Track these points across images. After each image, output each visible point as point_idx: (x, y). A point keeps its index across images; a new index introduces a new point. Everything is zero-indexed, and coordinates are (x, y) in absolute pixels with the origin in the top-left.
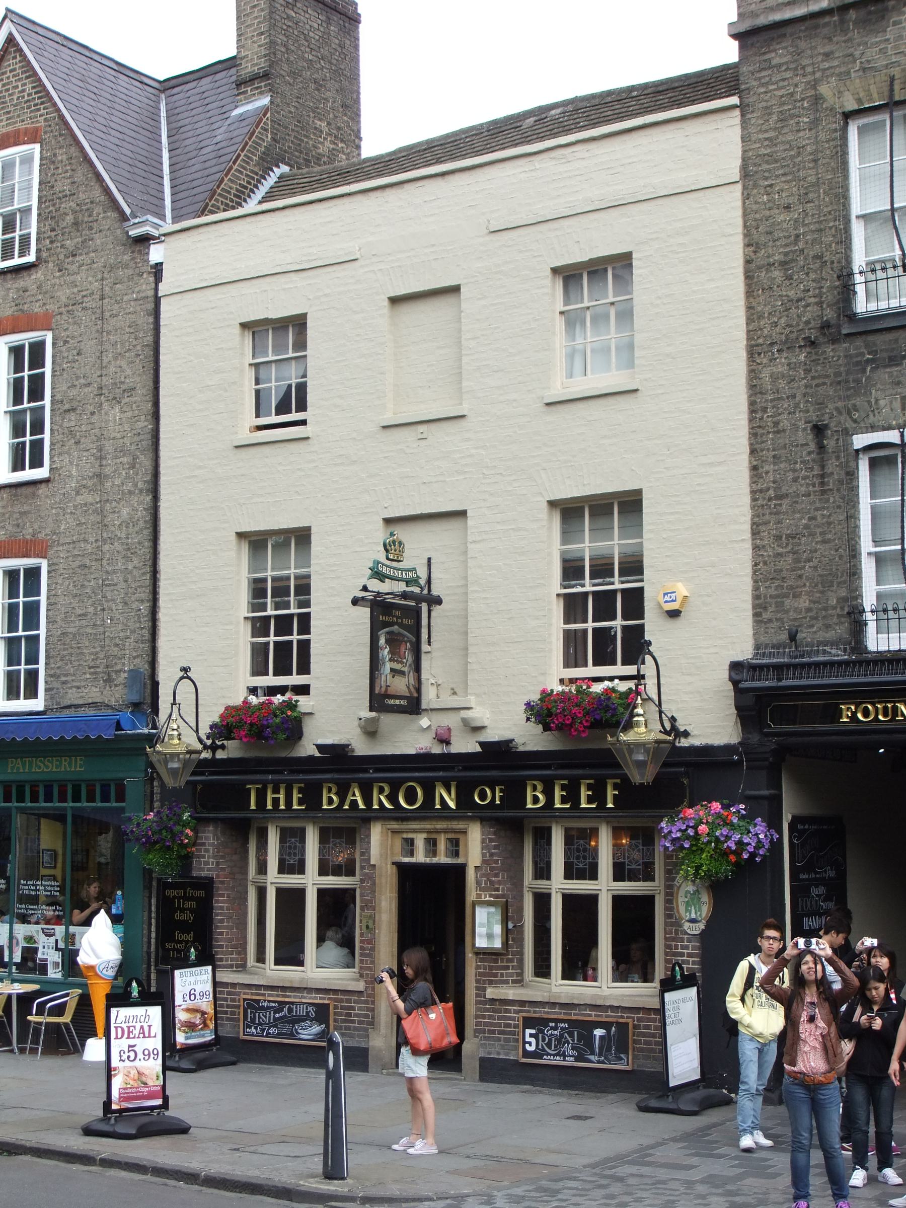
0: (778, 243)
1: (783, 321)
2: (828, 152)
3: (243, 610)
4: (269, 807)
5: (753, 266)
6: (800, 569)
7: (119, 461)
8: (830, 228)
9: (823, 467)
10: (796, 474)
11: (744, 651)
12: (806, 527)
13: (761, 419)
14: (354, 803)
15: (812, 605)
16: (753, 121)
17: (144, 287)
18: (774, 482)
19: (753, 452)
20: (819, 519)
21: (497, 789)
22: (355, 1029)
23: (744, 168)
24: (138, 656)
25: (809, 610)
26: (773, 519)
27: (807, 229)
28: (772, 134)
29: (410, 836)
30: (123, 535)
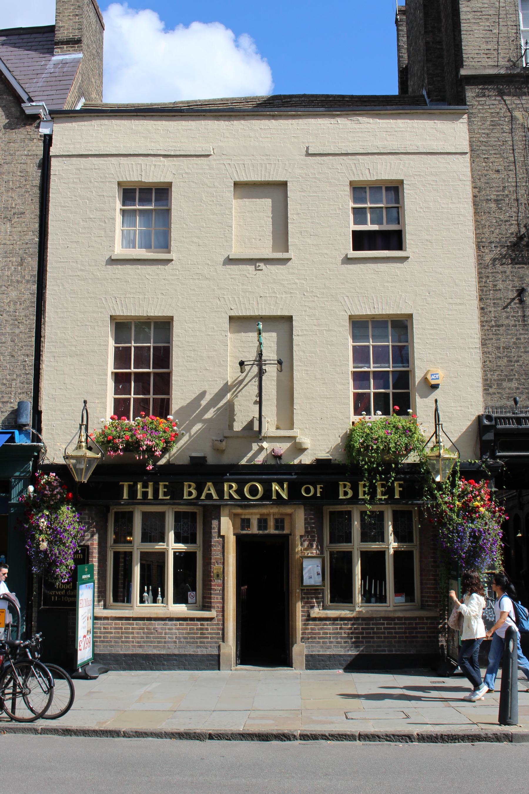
0: (493, 189)
1: (497, 231)
2: (521, 147)
3: (111, 368)
4: (139, 496)
5: (478, 199)
6: (512, 366)
7: (9, 259)
8: (523, 186)
9: (524, 312)
10: (508, 314)
11: (480, 411)
12: (514, 343)
13: (486, 282)
14: (209, 496)
15: (519, 386)
16: (475, 123)
17: (34, 148)
18: (495, 317)
19: (481, 299)
20: (522, 340)
21: (318, 486)
22: (208, 642)
23: (471, 146)
24: (23, 393)
25: (518, 388)
26: (494, 337)
27: (510, 185)
28: (487, 131)
29: (247, 517)
30: (11, 310)
